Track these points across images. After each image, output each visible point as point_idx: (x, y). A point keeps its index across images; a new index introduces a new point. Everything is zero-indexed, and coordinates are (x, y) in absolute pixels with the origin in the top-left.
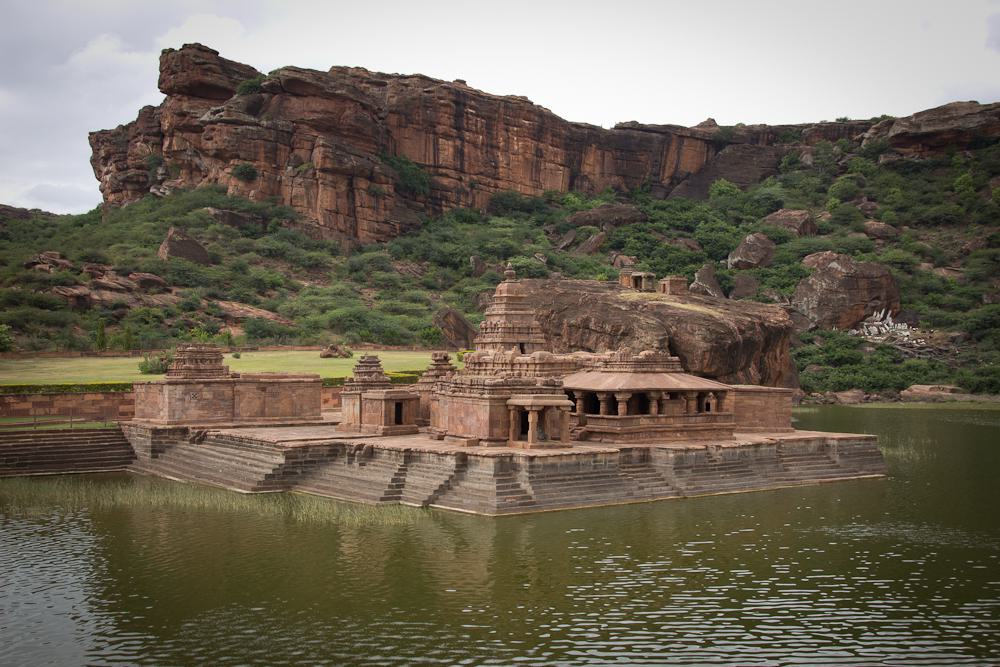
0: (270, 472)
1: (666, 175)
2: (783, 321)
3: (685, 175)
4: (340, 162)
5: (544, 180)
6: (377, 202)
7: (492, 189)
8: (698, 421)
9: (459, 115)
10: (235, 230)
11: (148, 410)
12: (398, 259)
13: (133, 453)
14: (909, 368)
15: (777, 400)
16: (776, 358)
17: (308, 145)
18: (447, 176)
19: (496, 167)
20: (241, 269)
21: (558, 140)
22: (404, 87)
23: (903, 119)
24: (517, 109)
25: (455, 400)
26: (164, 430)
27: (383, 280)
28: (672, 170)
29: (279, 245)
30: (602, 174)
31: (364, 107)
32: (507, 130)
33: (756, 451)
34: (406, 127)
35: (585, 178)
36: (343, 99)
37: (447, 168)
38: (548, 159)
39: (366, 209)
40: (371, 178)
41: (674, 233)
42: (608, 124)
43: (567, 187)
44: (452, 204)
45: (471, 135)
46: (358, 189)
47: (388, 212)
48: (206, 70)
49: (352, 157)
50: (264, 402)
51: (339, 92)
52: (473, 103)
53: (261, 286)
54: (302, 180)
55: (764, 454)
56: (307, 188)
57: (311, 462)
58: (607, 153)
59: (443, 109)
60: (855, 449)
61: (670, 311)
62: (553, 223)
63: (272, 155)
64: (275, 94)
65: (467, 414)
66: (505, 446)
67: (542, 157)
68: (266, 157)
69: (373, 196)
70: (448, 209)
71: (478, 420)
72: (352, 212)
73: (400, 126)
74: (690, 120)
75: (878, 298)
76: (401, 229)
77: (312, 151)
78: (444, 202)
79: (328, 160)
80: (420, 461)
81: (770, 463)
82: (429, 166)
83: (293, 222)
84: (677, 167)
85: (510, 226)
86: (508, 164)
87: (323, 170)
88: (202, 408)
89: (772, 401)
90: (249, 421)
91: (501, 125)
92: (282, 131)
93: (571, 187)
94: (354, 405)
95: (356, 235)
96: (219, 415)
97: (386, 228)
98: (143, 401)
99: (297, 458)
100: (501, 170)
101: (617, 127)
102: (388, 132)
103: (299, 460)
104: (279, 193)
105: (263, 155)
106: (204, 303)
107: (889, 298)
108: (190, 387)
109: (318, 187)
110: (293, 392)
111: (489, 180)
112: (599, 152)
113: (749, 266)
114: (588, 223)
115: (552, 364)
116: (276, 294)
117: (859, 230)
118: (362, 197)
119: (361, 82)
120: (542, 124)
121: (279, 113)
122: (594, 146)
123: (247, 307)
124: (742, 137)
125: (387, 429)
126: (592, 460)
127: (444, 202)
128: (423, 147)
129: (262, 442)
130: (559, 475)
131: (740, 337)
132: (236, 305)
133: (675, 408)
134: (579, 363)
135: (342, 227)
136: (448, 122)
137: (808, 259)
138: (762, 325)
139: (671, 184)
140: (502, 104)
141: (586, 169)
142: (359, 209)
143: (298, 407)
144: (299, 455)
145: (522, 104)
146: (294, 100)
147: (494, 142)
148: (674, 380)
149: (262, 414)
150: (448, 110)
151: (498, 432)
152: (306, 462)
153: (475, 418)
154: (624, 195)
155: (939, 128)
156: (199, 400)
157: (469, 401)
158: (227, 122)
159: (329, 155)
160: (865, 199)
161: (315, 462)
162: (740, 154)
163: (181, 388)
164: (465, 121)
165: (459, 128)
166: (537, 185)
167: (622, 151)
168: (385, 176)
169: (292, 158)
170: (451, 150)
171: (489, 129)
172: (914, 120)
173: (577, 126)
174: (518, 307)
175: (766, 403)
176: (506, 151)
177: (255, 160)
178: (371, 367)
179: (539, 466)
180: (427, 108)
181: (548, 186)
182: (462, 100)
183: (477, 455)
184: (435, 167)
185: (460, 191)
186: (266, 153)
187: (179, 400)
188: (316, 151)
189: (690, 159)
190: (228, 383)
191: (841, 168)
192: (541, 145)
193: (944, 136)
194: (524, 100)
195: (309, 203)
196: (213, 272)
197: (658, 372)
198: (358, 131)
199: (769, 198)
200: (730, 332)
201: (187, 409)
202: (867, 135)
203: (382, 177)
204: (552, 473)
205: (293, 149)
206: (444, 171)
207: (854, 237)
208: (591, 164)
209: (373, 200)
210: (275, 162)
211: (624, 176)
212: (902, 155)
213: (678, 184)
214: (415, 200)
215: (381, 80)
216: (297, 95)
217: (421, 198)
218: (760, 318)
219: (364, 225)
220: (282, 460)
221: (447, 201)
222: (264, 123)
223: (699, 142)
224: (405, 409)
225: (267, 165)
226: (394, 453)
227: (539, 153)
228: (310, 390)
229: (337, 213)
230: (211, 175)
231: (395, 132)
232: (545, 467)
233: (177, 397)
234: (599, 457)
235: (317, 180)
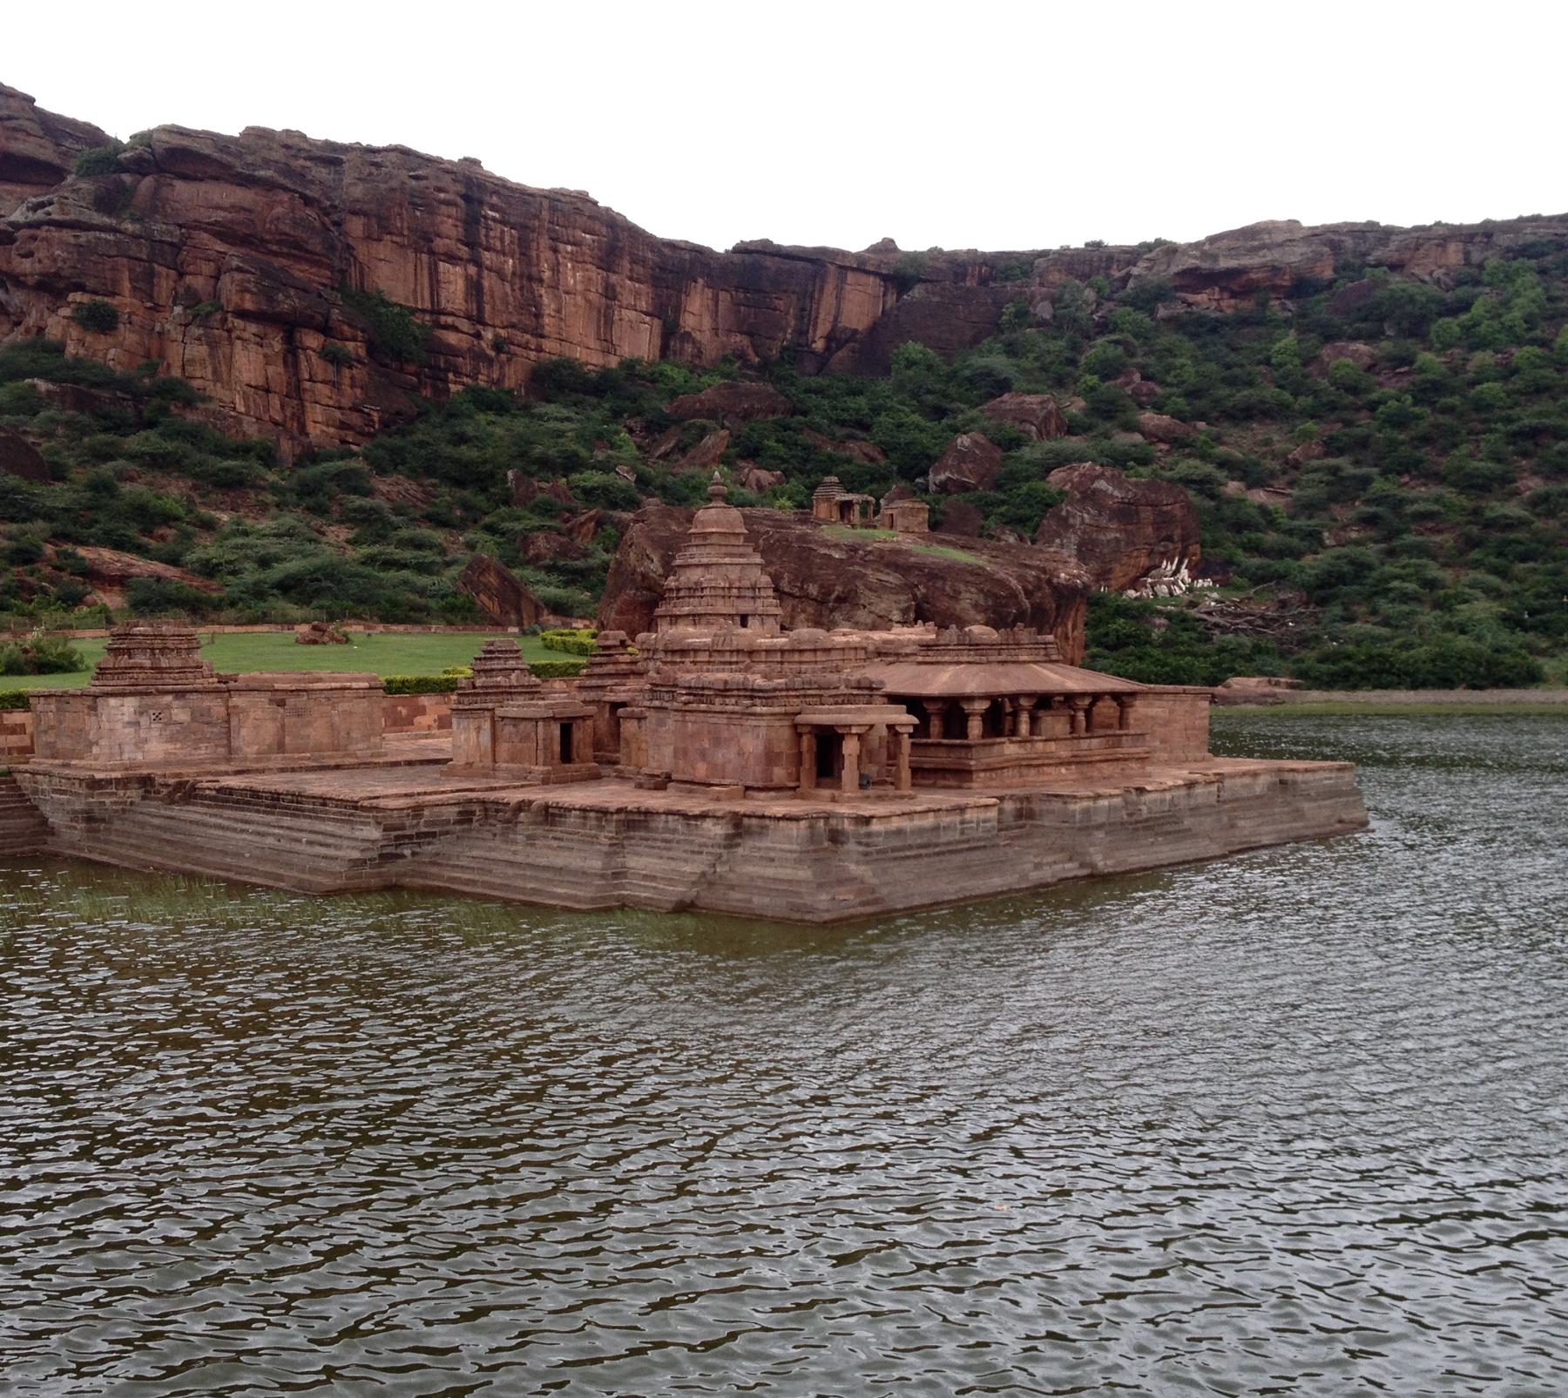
0: (356, 855)
1: (819, 333)
2: (1079, 576)
3: (849, 333)
4: (270, 300)
5: (620, 339)
6: (339, 372)
7: (533, 355)
8: (1092, 745)
9: (472, 222)
10: (85, 419)
11: (65, 743)
12: (382, 472)
13: (44, 821)
14: (1222, 650)
15: (1186, 706)
16: (1067, 638)
17: (208, 268)
18: (455, 329)
19: (538, 316)
20: (102, 487)
21: (641, 270)
22: (373, 169)
23: (1190, 245)
24: (570, 211)
25: (689, 717)
26: (109, 782)
27: (361, 510)
28: (828, 327)
29: (169, 446)
30: (715, 330)
31: (308, 201)
32: (555, 250)
34: (379, 240)
35: (687, 337)
36: (269, 186)
37: (452, 314)
38: (625, 303)
39: (319, 385)
40: (325, 329)
41: (840, 432)
42: (721, 243)
43: (658, 354)
44: (465, 380)
45: (494, 255)
46: (305, 349)
47: (358, 391)
48: (15, 129)
49: (292, 292)
50: (283, 726)
51: (262, 173)
52: (495, 199)
53: (148, 517)
54: (201, 331)
56: (213, 345)
57: (427, 835)
58: (723, 296)
59: (444, 208)
61: (913, 559)
62: (639, 414)
63: (145, 285)
64: (145, 175)
65: (717, 742)
66: (795, 797)
67: (614, 298)
68: (134, 289)
69: (332, 362)
70: (460, 388)
71: (741, 753)
72: (296, 391)
73: (368, 237)
74: (854, 240)
75: (1169, 539)
76: (381, 421)
77: (217, 278)
78: (451, 376)
79: (248, 296)
80: (647, 829)
81: (1209, 815)
82: (423, 311)
83: (189, 403)
84: (836, 318)
85: (568, 419)
86: (559, 311)
87: (242, 314)
88: (172, 739)
90: (258, 760)
91: (545, 241)
92: (161, 242)
93: (664, 350)
94: (479, 729)
95: (303, 430)
96: (203, 752)
97: (355, 419)
98: (52, 728)
99: (403, 828)
100: (547, 320)
101: (742, 249)
102: (349, 248)
103: (408, 832)
104: (162, 356)
105: (127, 285)
106: (49, 549)
107: (1184, 539)
108: (148, 700)
109: (231, 344)
110: (334, 708)
111: (528, 336)
112: (709, 293)
113: (965, 487)
114: (697, 414)
115: (827, 650)
116: (171, 533)
117: (1129, 427)
118: (312, 364)
119: (296, 157)
120: (615, 241)
121: (154, 210)
122: (700, 281)
123: (127, 558)
124: (940, 270)
125: (548, 772)
126: (958, 818)
127: (451, 376)
128: (412, 278)
129: (324, 801)
130: (910, 847)
131: (1026, 603)
132: (107, 554)
133: (1054, 724)
134: (871, 648)
135: (278, 418)
136: (453, 233)
137: (1056, 476)
138: (1049, 582)
139: (827, 348)
140: (546, 203)
141: (688, 322)
142: (307, 385)
143: (343, 734)
144: (408, 823)
145: (579, 205)
146: (178, 184)
147: (534, 270)
148: (1052, 675)
149: (281, 747)
150: (453, 211)
151: (780, 774)
152: (419, 835)
153: (734, 750)
154: (751, 367)
155: (1246, 261)
156: (166, 724)
157: (723, 720)
158: (60, 225)
159: (251, 286)
160: (1137, 377)
161: (433, 835)
162: (936, 299)
163: (131, 703)
164: (483, 231)
165: (471, 244)
166: (608, 347)
167: (746, 290)
168: (350, 325)
169: (181, 290)
170: (461, 283)
171: (524, 248)
172: (1207, 247)
173: (672, 245)
174: (735, 550)
175: (1171, 712)
176: (554, 286)
177: (113, 294)
178: (507, 659)
179: (878, 834)
180: (415, 206)
181: (626, 351)
182: (476, 195)
183: (763, 817)
184: (432, 312)
185: (479, 356)
186: (131, 280)
187: (129, 723)
188: (226, 278)
189: (858, 307)
190: (217, 691)
191: (1097, 325)
192: (614, 278)
193: (1253, 276)
194: (583, 197)
195: (215, 372)
196: (58, 495)
197: (1025, 662)
198: (297, 245)
199: (988, 373)
200: (1013, 595)
201: (146, 741)
202: (1135, 271)
203: (346, 328)
205: (181, 275)
206: (450, 320)
207: (1123, 440)
208: (697, 312)
209: (331, 368)
210: (151, 298)
211: (750, 334)
212: (1190, 305)
213: (839, 348)
214: (401, 370)
215: (332, 155)
216: (185, 177)
217: (412, 368)
218: (1044, 570)
219: (315, 414)
220: (374, 833)
221: (458, 373)
222: (129, 227)
223: (872, 279)
224: (577, 735)
225: (137, 303)
226: (592, 815)
227: (610, 293)
228: (364, 704)
229: (268, 391)
230: (31, 321)
231: (361, 251)
232: (888, 834)
233: (126, 719)
235: (229, 331)
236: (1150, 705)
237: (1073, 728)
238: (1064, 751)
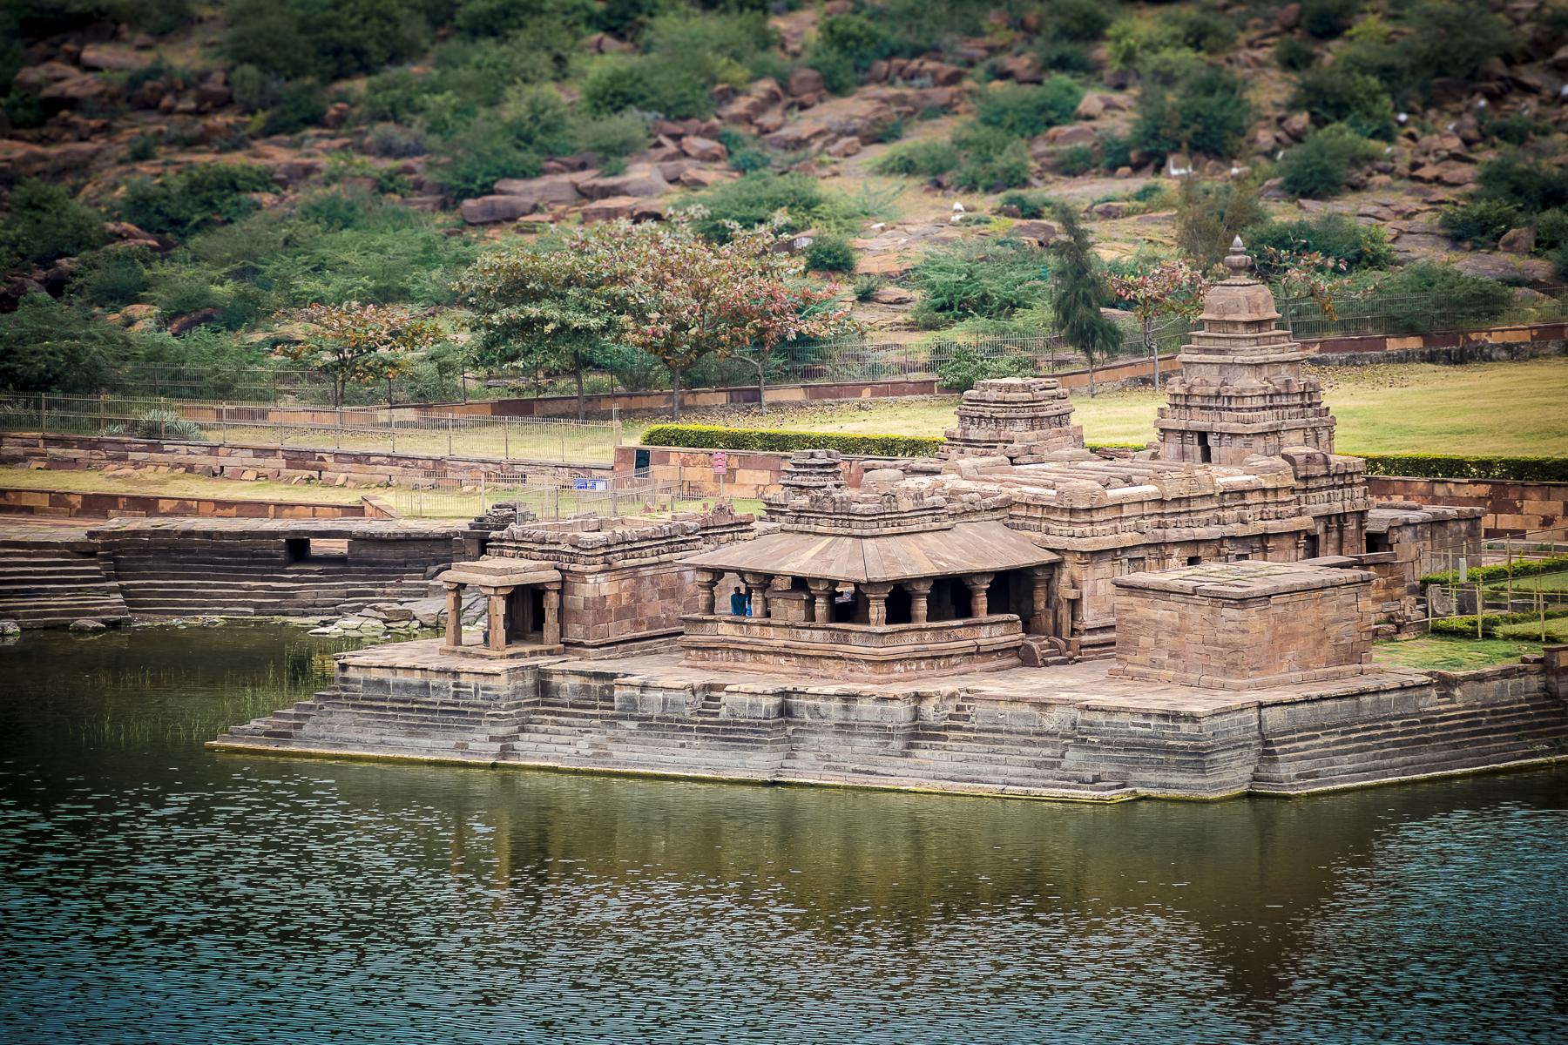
55: (865, 716)
60: (1132, 734)
81: (871, 736)
126: (451, 682)
175: (1182, 617)
179: (357, 681)
204: (380, 694)
232: (367, 683)
234: (463, 679)
237: (811, 616)
238: (778, 639)
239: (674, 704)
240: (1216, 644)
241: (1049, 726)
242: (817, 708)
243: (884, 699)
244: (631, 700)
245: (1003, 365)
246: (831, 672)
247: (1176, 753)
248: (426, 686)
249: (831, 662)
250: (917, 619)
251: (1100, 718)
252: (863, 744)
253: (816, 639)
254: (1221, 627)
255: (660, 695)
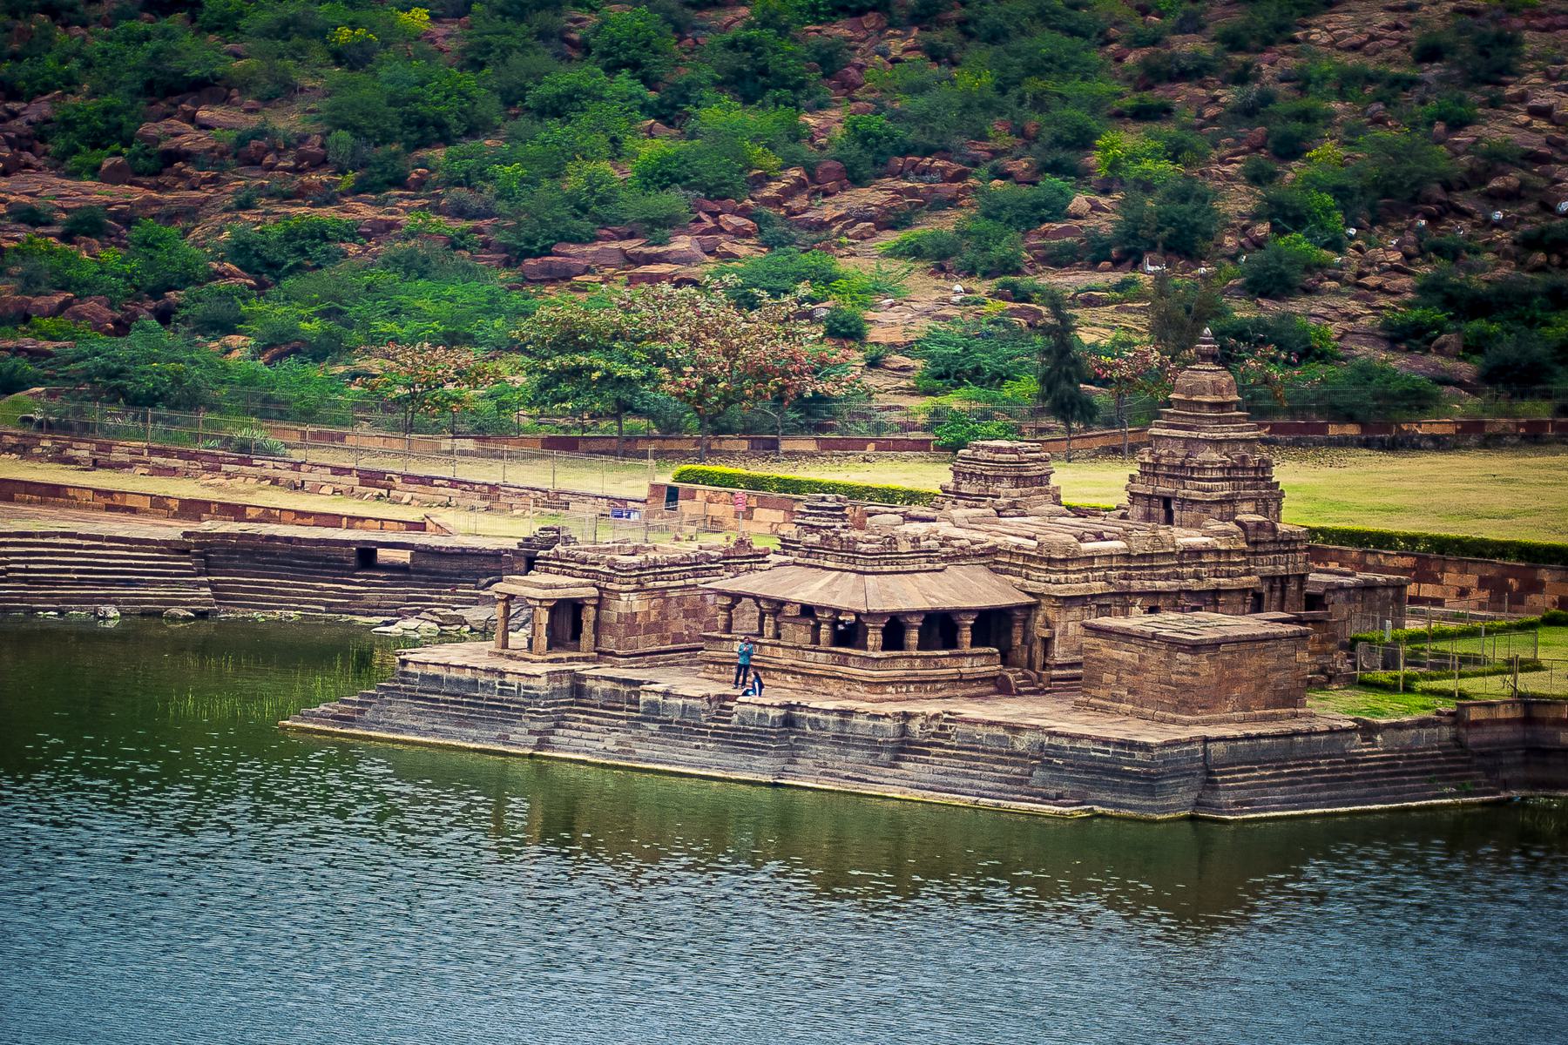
33: (842, 722)
81: (863, 748)
89: (1153, 658)
126: (497, 680)
175: (1141, 659)
179: (415, 675)
204: (434, 688)
232: (424, 677)
234: (509, 678)
236: (1116, 647)
237: (816, 640)
239: (692, 710)
240: (1170, 684)
241: (1020, 747)
242: (817, 720)
243: (876, 717)
244: (654, 704)
245: (992, 429)
246: (831, 689)
247: (1129, 778)
248: (476, 682)
249: (832, 682)
250: (909, 648)
251: (1065, 743)
252: (856, 755)
253: (819, 661)
254: (1175, 669)
255: (680, 702)
